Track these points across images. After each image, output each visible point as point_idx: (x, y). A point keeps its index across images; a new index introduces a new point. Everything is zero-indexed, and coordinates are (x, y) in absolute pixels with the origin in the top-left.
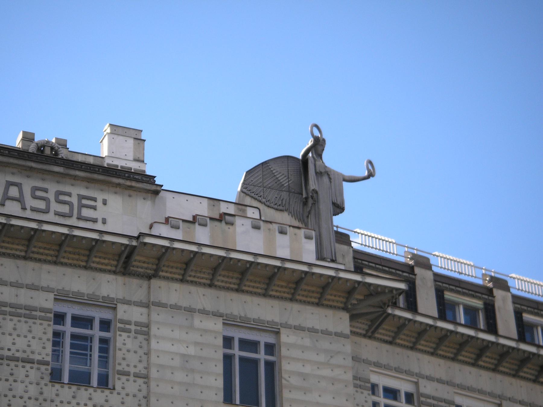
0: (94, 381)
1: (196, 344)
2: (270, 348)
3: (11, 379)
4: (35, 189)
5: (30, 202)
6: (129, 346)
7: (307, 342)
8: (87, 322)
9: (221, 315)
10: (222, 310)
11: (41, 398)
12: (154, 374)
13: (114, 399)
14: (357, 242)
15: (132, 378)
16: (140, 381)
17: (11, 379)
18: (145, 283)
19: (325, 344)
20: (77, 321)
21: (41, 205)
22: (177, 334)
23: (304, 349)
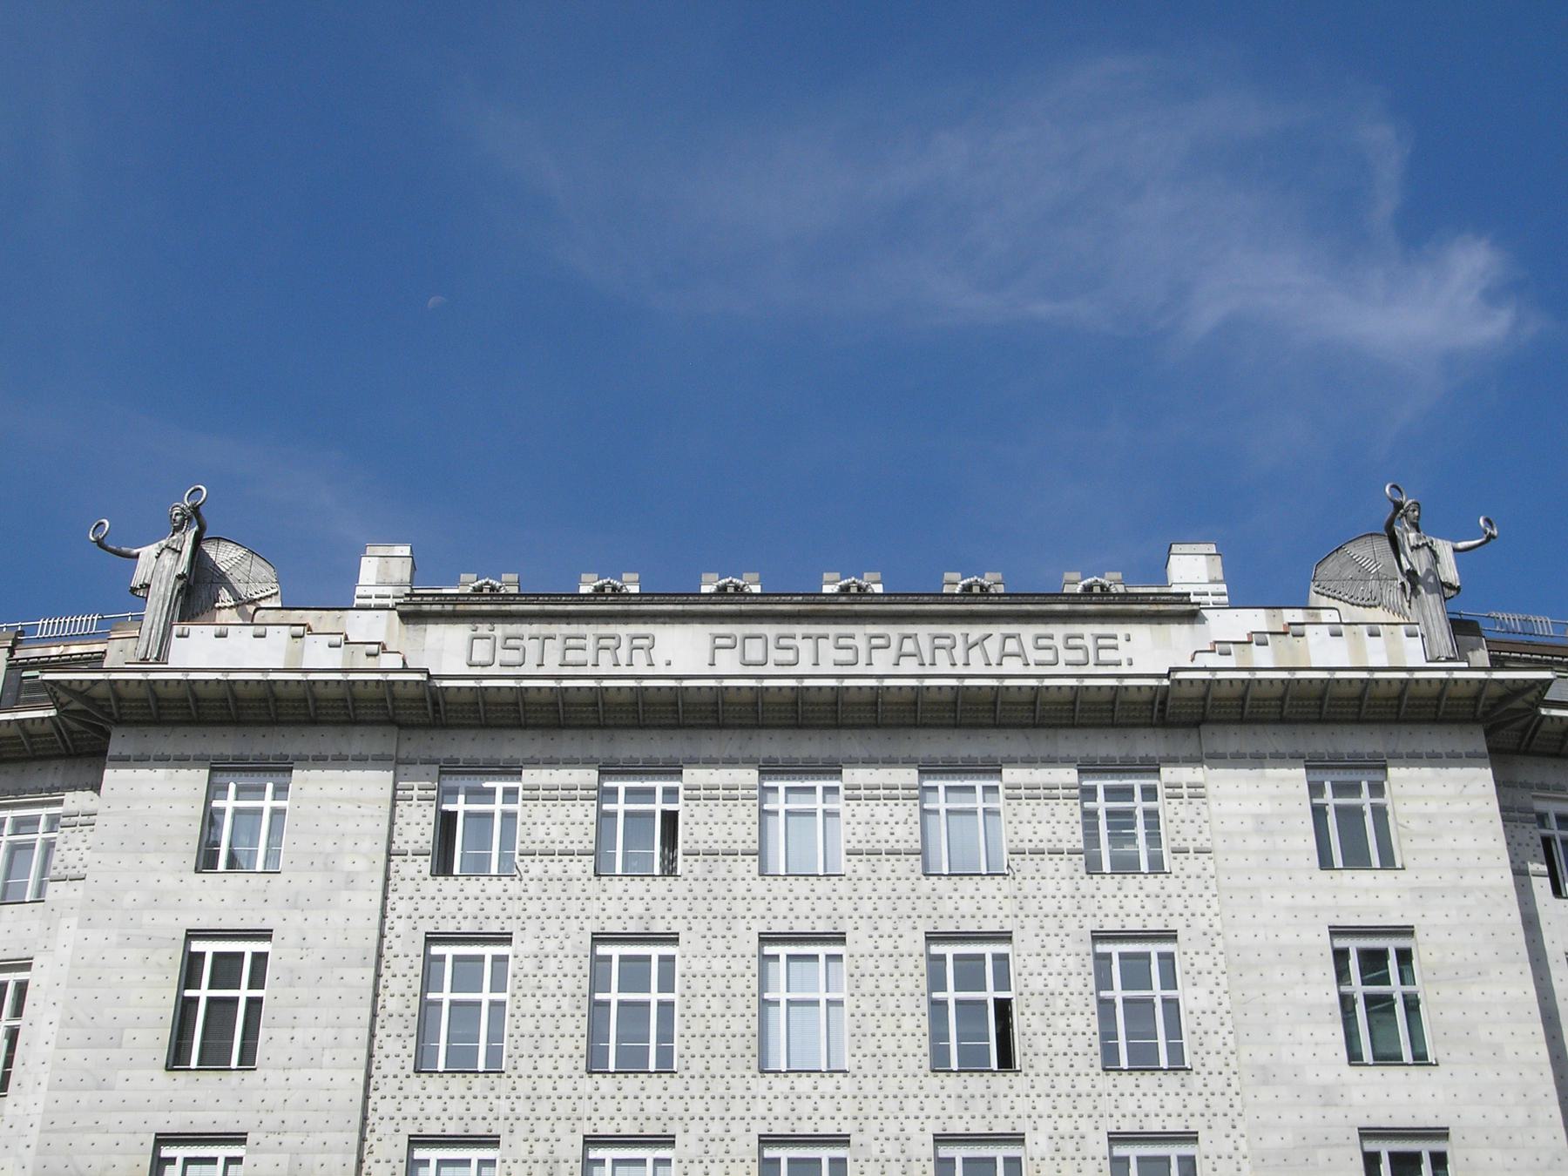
0: (1144, 867)
1: (1272, 798)
3: (1038, 876)
4: (1039, 637)
5: (1033, 655)
6: (1182, 815)
8: (1127, 793)
9: (1301, 757)
10: (1302, 749)
11: (1078, 895)
12: (1218, 844)
13: (1172, 885)
15: (1192, 855)
16: (1203, 857)
17: (1038, 876)
18: (1195, 731)
20: (1111, 793)
21: (1048, 656)
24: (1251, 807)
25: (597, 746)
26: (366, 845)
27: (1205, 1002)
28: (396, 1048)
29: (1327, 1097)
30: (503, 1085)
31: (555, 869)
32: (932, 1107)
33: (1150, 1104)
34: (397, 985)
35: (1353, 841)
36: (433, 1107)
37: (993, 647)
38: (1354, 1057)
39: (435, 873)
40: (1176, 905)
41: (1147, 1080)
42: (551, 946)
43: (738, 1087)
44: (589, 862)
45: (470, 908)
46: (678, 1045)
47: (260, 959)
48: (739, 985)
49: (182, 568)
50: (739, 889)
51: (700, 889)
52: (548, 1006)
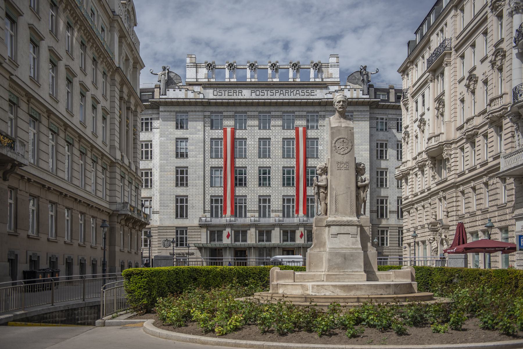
5: (301, 94)
7: (359, 114)
13: (319, 131)
19: (364, 114)
21: (303, 94)
23: (358, 115)
25: (234, 109)
28: (208, 154)
32: (282, 163)
33: (313, 163)
36: (214, 163)
37: (295, 92)
39: (211, 129)
40: (319, 134)
43: (255, 160)
45: (216, 134)
46: (247, 154)
48: (256, 146)
49: (166, 78)
50: (256, 131)
51: (250, 131)
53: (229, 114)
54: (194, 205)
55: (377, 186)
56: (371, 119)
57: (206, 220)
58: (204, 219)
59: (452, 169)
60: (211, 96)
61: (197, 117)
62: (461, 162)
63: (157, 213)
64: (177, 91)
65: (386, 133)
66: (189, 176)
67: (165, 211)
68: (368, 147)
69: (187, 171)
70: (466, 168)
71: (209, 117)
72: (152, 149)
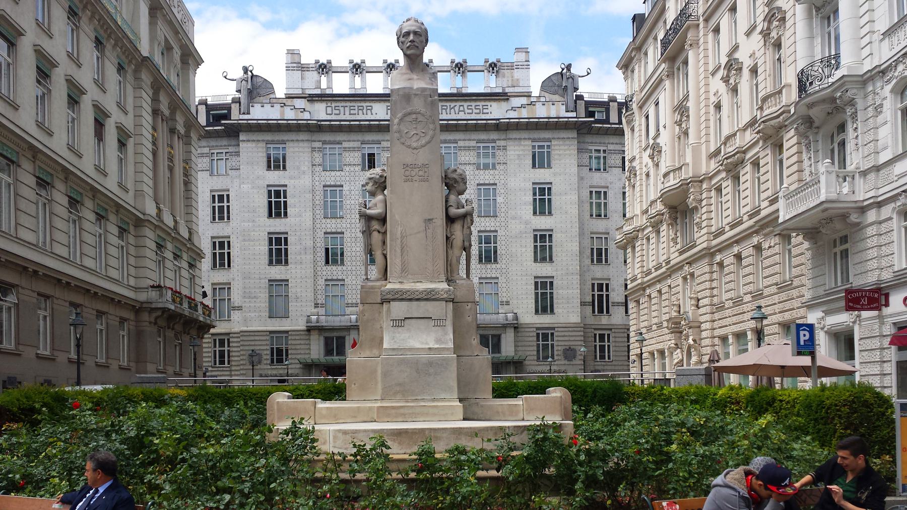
2: (549, 147)
5: (467, 111)
13: (497, 172)
14: (587, 98)
19: (568, 142)
21: (470, 111)
22: (516, 148)
24: (517, 153)
25: (360, 137)
26: (306, 163)
27: (502, 200)
28: (320, 212)
29: (527, 223)
30: (344, 221)
31: (352, 169)
33: (488, 224)
34: (317, 198)
35: (540, 161)
36: (329, 226)
37: (457, 109)
38: (535, 213)
40: (497, 177)
41: (487, 219)
42: (352, 188)
44: (360, 167)
45: (333, 179)
47: (285, 191)
52: (353, 202)
53: (351, 144)
54: (299, 295)
55: (592, 261)
56: (580, 151)
57: (318, 319)
58: (314, 318)
59: (704, 224)
60: (322, 116)
61: (301, 149)
62: (719, 214)
63: (239, 308)
64: (267, 107)
65: (605, 175)
66: (289, 247)
67: (252, 305)
68: (575, 198)
69: (286, 239)
70: (726, 221)
71: (320, 150)
72: (230, 204)
